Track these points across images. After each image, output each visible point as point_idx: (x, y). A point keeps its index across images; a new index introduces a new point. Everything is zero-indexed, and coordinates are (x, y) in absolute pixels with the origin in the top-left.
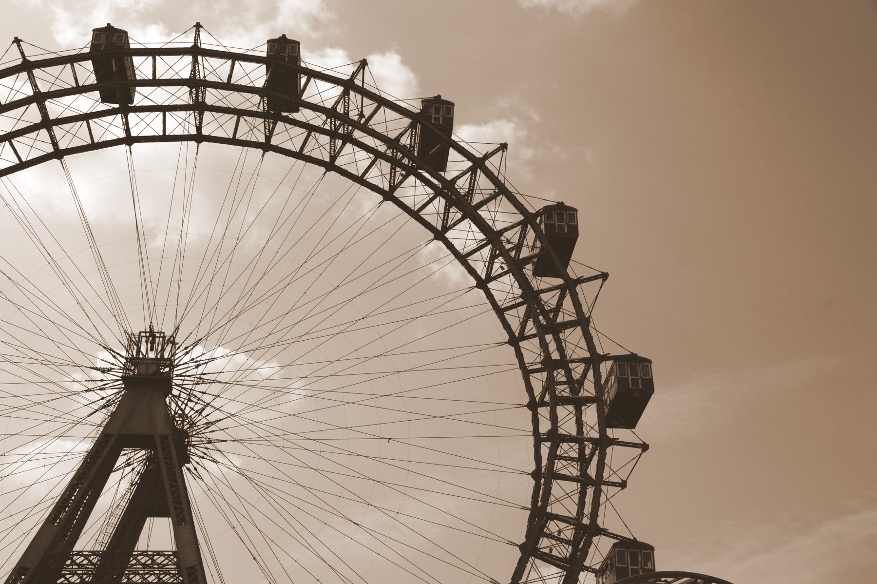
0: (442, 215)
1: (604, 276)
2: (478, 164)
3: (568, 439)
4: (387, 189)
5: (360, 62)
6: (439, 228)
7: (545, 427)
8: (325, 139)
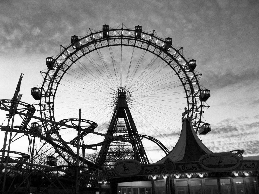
1: (209, 107)
4: (177, 72)
6: (184, 83)
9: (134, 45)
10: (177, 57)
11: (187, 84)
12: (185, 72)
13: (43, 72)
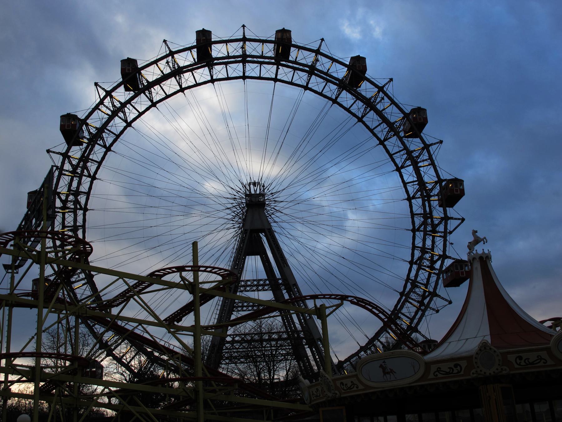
2: (426, 147)
5: (390, 79)
6: (400, 166)
9: (274, 76)
10: (378, 103)
11: (407, 166)
12: (401, 139)
13: (54, 152)
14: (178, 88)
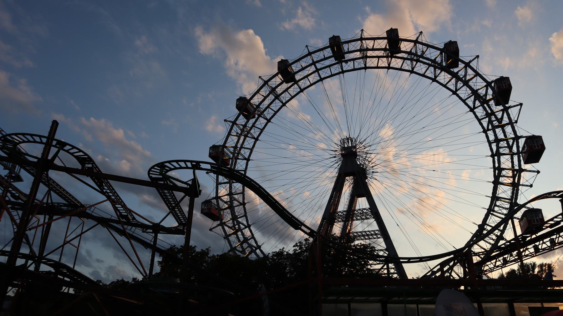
0: (433, 73)
3: (502, 140)
6: (433, 77)
7: (492, 138)
8: (385, 59)
14: (266, 121)
